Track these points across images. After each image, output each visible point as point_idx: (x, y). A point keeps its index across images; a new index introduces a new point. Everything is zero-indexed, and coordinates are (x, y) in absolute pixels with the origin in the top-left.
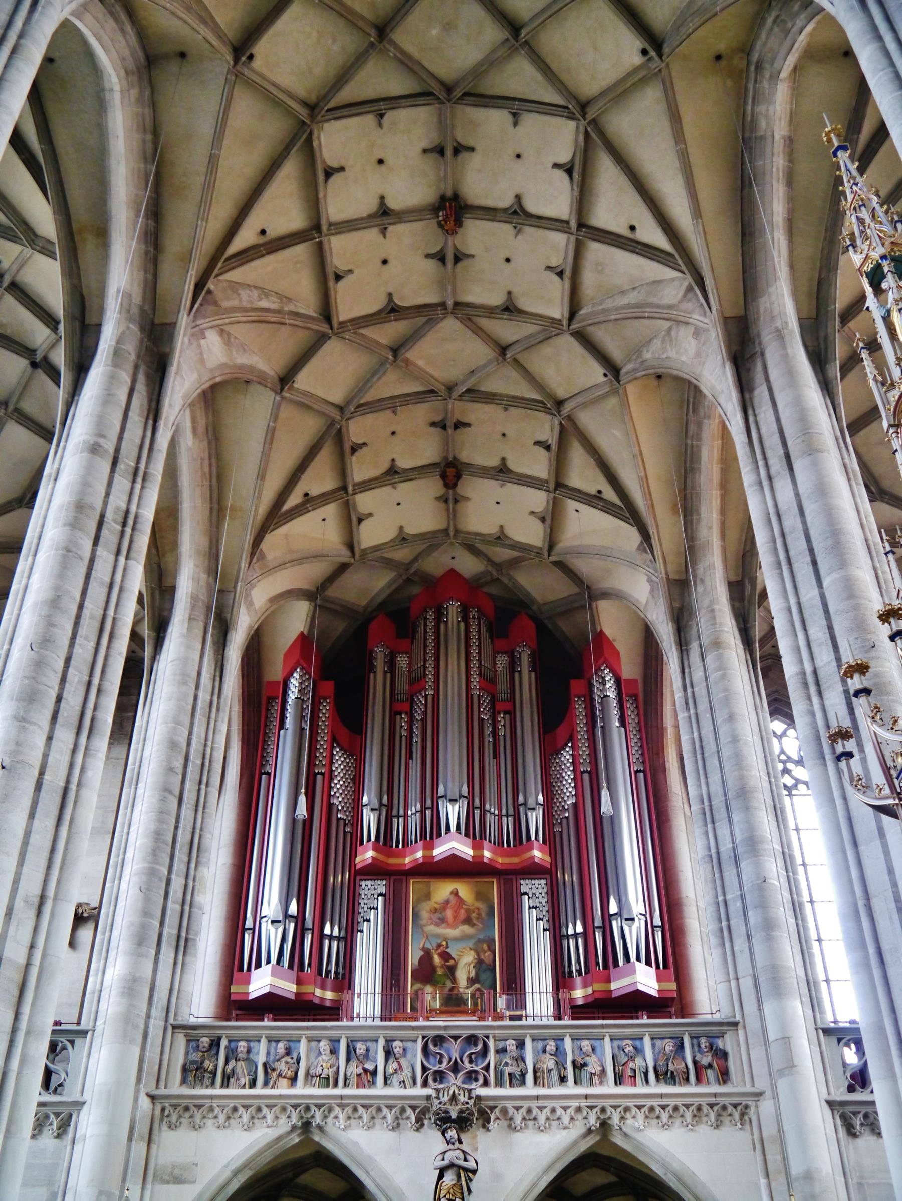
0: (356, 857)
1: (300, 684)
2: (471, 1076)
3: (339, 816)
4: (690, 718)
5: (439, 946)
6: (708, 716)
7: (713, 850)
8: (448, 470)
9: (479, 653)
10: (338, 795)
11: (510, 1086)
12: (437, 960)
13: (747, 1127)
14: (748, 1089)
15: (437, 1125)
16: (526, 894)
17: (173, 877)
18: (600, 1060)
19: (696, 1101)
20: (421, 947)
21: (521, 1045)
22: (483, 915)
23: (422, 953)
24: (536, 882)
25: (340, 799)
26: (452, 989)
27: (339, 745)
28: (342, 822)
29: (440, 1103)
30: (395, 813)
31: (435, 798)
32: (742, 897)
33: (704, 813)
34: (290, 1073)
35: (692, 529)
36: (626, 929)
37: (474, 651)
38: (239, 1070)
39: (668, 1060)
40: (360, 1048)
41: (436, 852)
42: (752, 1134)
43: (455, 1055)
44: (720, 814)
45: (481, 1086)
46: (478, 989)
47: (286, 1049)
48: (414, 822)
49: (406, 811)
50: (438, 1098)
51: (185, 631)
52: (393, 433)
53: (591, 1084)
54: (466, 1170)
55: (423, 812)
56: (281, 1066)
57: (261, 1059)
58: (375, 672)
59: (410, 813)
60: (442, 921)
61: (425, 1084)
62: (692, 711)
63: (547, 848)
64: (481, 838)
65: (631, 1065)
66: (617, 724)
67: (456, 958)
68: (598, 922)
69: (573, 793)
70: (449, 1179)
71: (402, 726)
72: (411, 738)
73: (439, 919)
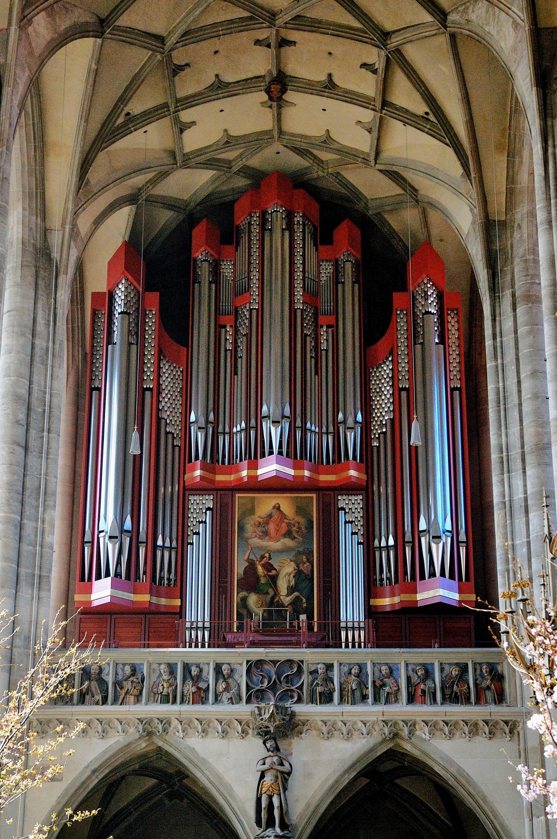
0: (184, 473)
1: (126, 296)
2: (287, 695)
3: (168, 430)
4: (497, 367)
5: (263, 557)
6: (514, 368)
7: (507, 499)
8: (272, 86)
9: (304, 263)
10: (166, 409)
11: (320, 703)
12: (260, 570)
13: (516, 738)
14: (519, 708)
15: (260, 734)
16: (343, 509)
17: (25, 521)
18: (397, 682)
19: (474, 718)
20: (246, 558)
21: (329, 667)
22: (303, 529)
23: (247, 564)
24: (353, 498)
25: (168, 413)
26: (273, 598)
27: (164, 357)
28: (170, 436)
29: (262, 720)
30: (220, 429)
31: (260, 419)
32: (529, 543)
33: (502, 462)
34: (136, 692)
35: (513, 171)
36: (434, 546)
37: (298, 260)
38: (93, 689)
39: (453, 683)
40: (194, 671)
41: (260, 472)
42: (519, 745)
43: (274, 677)
44: (517, 465)
45: (296, 702)
46: (297, 597)
47: (132, 670)
48: (239, 439)
49: (231, 428)
50: (260, 715)
51: (19, 279)
52: (216, 52)
53: (387, 702)
54: (282, 773)
55: (247, 430)
56: (128, 685)
57: (110, 680)
58: (199, 282)
59: (235, 430)
60: (266, 533)
61: (248, 701)
62: (499, 361)
63: (363, 465)
64: (301, 458)
65: (422, 686)
66: (437, 341)
67: (278, 568)
68: (408, 537)
69: (391, 409)
70: (269, 779)
71: (226, 339)
72: (236, 351)
73: (263, 532)
